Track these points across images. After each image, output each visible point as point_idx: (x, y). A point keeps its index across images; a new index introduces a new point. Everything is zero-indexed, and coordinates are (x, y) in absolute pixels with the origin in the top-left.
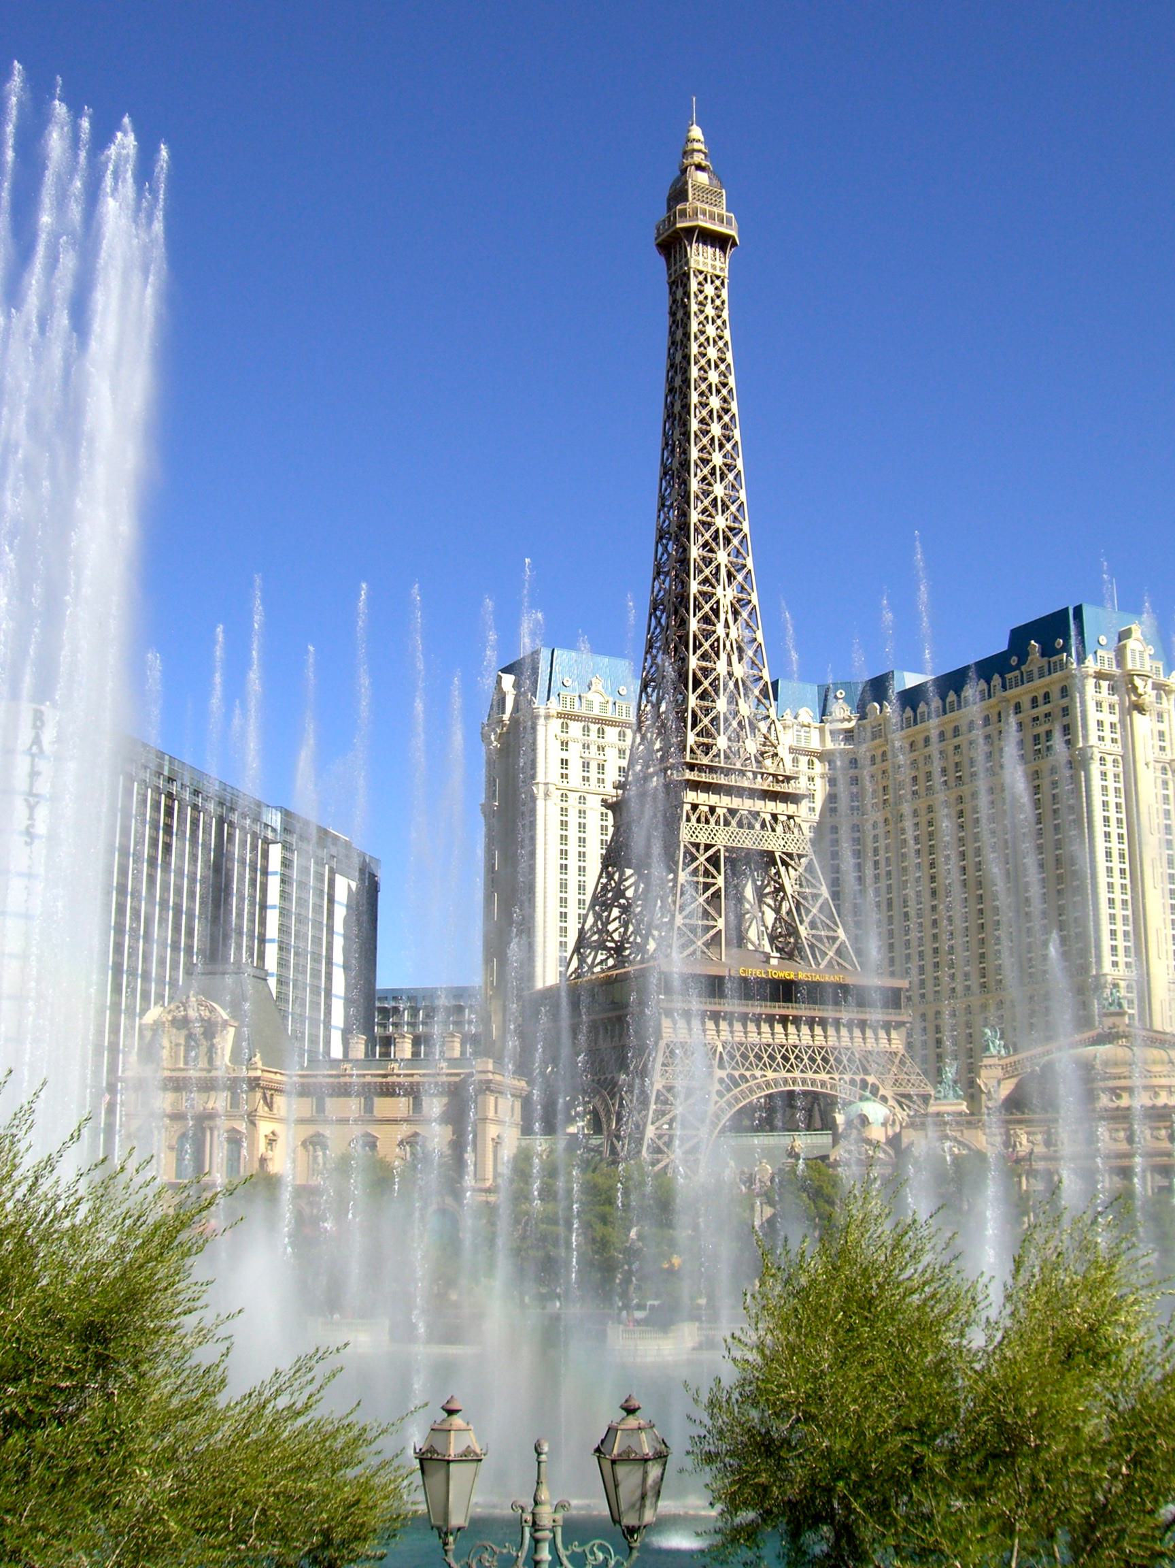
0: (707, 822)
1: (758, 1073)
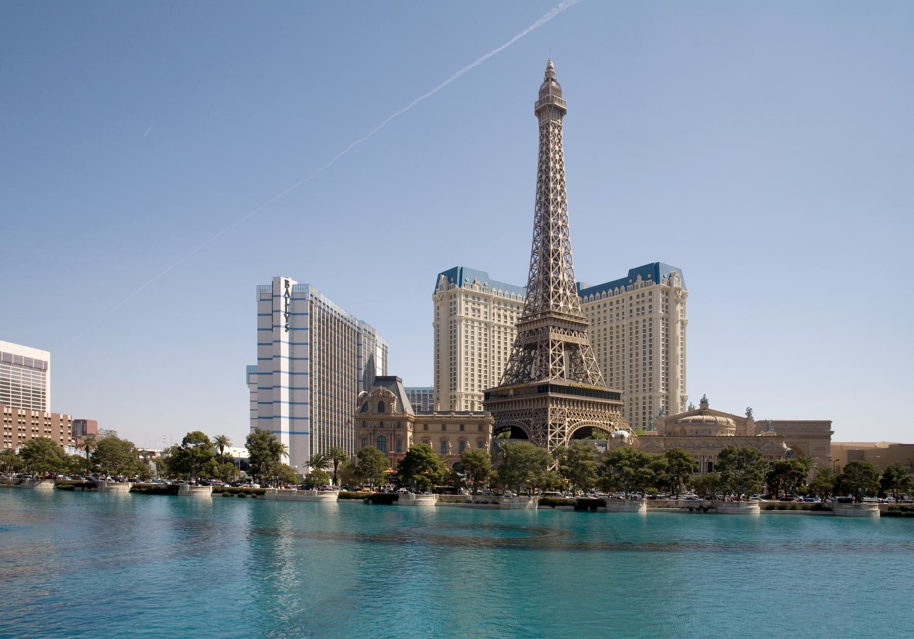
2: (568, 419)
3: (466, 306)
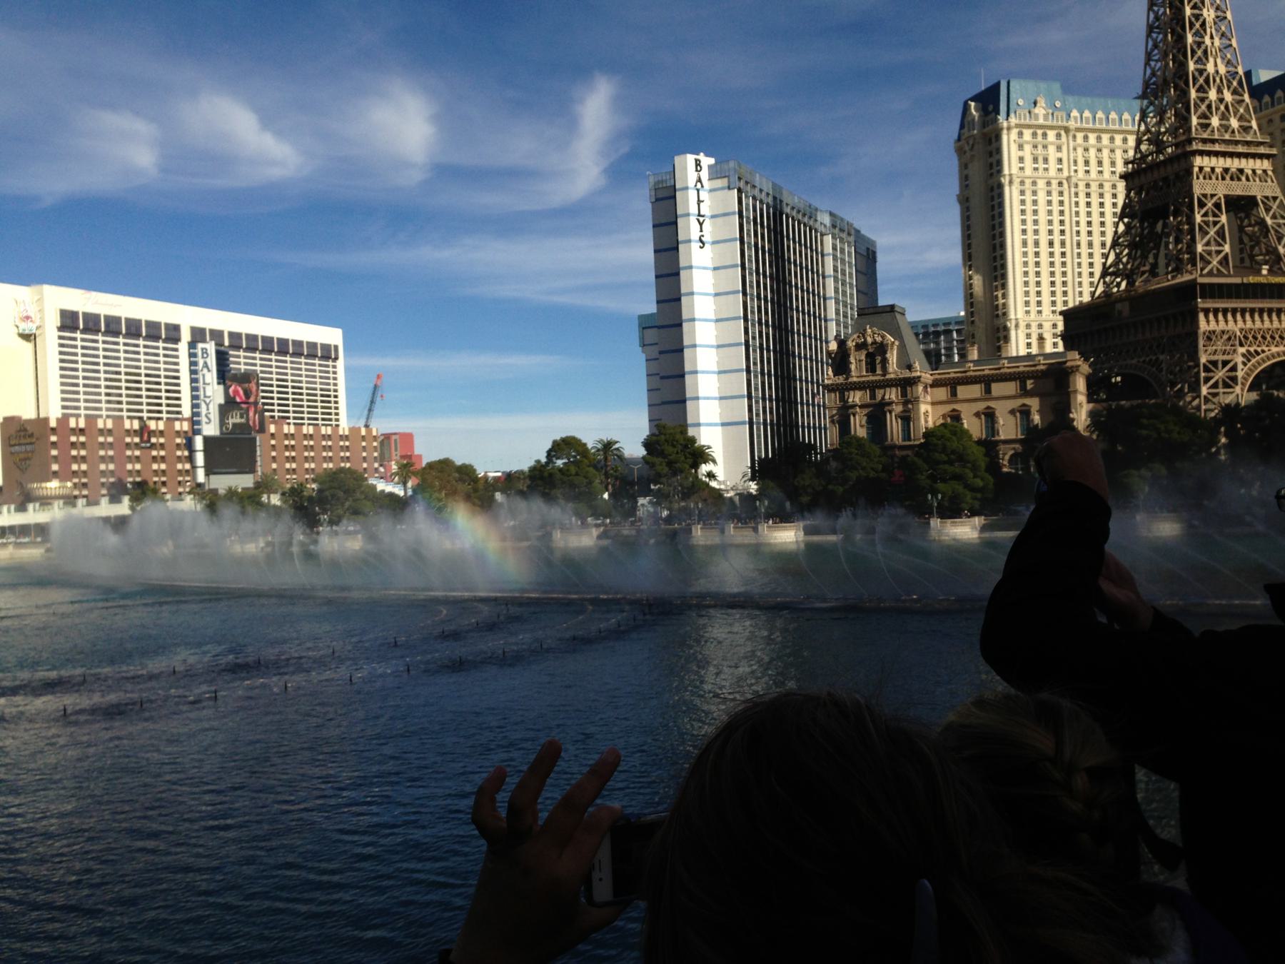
0: (1210, 178)
2: (1242, 350)
3: (1021, 153)
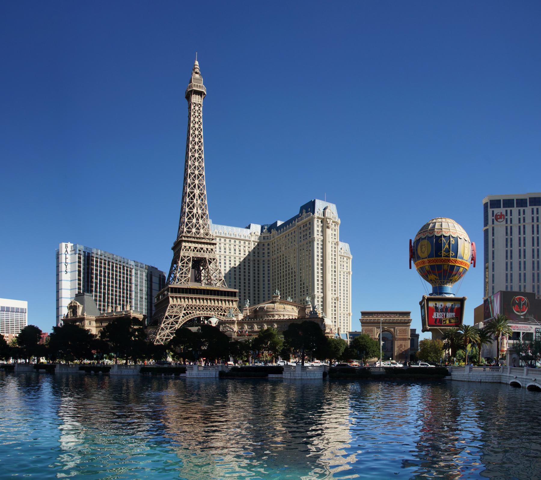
0: (188, 250)
1: (194, 312)
